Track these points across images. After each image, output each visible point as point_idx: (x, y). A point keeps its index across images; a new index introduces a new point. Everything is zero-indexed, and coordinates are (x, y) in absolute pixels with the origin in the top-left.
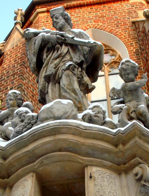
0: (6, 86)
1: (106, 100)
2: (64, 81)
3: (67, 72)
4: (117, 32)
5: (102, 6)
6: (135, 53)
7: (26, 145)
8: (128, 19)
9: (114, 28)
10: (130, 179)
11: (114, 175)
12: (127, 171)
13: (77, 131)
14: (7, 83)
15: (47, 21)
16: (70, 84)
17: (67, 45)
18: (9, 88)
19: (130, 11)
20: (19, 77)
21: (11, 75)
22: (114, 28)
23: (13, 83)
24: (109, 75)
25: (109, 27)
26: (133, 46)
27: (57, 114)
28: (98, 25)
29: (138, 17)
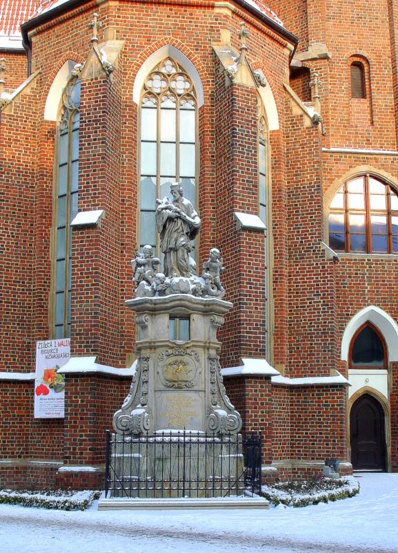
0: (88, 133)
1: (175, 143)
2: (180, 253)
3: (182, 248)
4: (196, 59)
5: (183, 9)
6: (210, 95)
7: (166, 303)
8: (210, 40)
9: (192, 52)
10: (207, 319)
11: (202, 317)
12: (207, 315)
13: (190, 301)
14: (89, 129)
15: (118, 17)
16: (183, 255)
17: (181, 219)
18: (92, 137)
19: (212, 27)
20: (103, 127)
21: (94, 121)
22: (192, 52)
23: (96, 132)
24: (181, 109)
25: (188, 48)
26: (209, 85)
27: (182, 289)
28: (177, 41)
29: (220, 41)
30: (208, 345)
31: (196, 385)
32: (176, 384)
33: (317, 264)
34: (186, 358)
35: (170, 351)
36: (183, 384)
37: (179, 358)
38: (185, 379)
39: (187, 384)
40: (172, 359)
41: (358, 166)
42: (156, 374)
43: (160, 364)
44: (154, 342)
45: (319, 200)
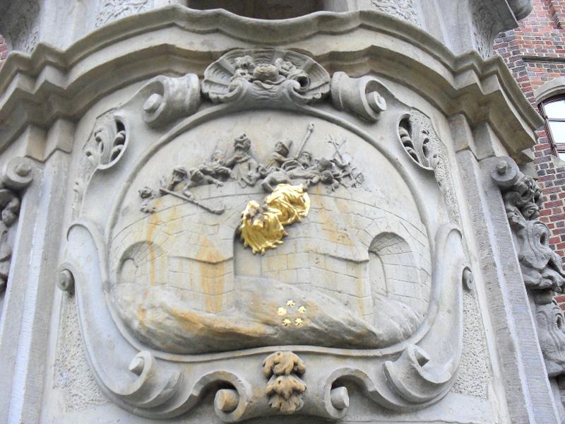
30: (471, 78)
31: (454, 383)
32: (246, 376)
33: (553, 197)
34: (324, 138)
35: (183, 85)
36: (321, 372)
37: (266, 133)
38: (339, 314)
39: (371, 374)
40: (199, 147)
41: (555, 78)
42: (60, 294)
43: (98, 209)
44: (65, 62)
45: (529, 84)
